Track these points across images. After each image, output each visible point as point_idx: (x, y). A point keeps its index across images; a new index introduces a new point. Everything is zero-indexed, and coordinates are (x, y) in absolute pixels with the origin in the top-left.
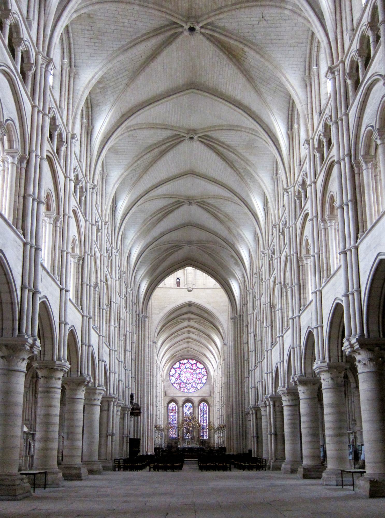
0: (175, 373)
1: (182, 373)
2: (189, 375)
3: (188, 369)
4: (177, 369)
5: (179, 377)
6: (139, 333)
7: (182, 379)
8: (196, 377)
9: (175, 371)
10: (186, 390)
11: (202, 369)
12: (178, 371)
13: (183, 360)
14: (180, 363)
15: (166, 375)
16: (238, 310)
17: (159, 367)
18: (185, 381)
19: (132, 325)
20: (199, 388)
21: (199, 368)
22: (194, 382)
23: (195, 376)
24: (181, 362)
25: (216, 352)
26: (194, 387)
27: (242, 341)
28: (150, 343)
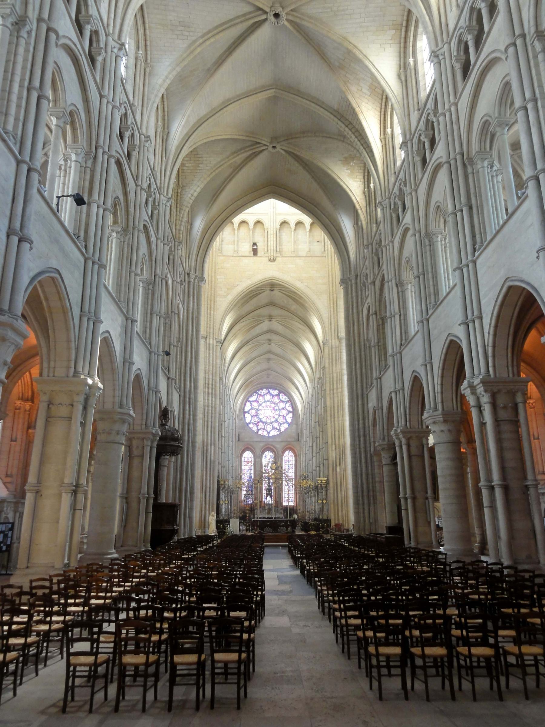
0: (252, 408)
1: (260, 408)
3: (268, 403)
4: (253, 403)
5: (257, 415)
6: (188, 307)
7: (261, 417)
9: (251, 405)
10: (265, 434)
12: (255, 405)
13: (262, 389)
14: (258, 394)
15: (240, 411)
16: (352, 269)
17: (228, 393)
18: (264, 420)
19: (173, 281)
20: (282, 429)
21: (283, 401)
22: (276, 421)
23: (277, 412)
24: (259, 393)
25: (307, 372)
26: (276, 429)
27: (361, 319)
28: (211, 342)
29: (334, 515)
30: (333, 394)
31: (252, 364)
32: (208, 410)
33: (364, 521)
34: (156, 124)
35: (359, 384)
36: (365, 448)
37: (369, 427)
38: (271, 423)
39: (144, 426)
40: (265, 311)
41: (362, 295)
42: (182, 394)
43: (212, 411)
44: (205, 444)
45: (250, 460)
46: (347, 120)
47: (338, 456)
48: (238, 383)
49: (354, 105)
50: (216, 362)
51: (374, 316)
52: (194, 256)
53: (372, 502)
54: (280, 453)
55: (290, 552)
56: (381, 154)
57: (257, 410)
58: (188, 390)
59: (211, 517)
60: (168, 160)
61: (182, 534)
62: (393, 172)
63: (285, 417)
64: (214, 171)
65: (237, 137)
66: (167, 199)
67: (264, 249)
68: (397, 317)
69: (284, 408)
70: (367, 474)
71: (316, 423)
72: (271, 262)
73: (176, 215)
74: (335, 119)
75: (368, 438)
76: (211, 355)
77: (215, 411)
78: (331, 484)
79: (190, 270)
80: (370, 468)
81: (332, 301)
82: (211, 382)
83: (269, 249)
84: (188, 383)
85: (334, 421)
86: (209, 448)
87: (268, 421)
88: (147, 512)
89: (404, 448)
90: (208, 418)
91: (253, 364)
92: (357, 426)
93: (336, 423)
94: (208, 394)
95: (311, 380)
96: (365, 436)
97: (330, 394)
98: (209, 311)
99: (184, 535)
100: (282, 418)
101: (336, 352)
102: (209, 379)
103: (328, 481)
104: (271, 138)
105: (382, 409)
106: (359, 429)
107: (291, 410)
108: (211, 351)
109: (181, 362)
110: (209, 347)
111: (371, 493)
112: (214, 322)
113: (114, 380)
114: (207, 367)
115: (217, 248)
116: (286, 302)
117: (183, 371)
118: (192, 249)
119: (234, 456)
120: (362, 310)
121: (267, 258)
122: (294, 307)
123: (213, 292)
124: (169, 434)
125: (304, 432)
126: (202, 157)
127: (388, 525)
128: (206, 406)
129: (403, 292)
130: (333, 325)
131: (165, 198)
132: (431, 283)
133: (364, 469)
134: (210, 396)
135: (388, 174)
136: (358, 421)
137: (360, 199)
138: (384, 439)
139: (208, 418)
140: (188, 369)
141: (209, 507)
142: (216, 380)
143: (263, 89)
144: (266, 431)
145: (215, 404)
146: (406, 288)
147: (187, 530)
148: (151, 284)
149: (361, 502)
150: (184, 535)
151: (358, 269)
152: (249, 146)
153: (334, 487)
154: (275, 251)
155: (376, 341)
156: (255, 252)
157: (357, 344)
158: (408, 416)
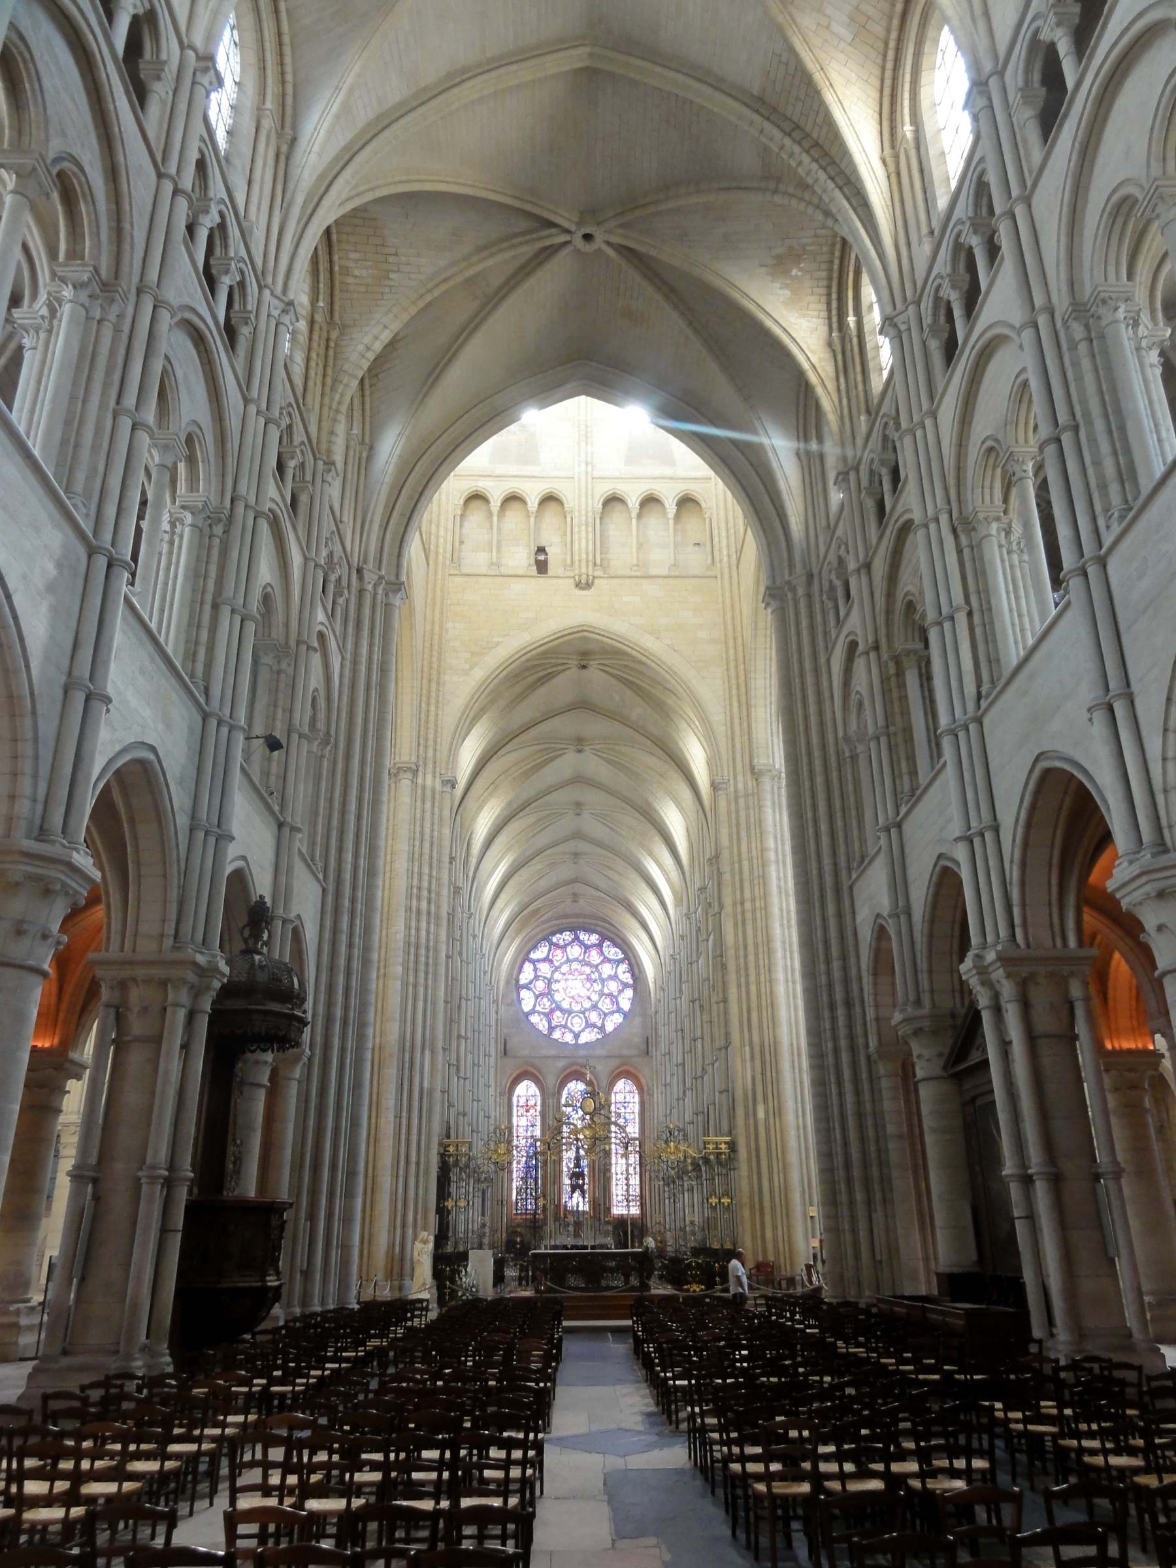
0: (536, 977)
1: (557, 976)
2: (578, 984)
3: (575, 965)
4: (540, 966)
5: (548, 993)
7: (557, 997)
8: (601, 990)
9: (536, 969)
10: (569, 1038)
11: (619, 962)
12: (545, 968)
13: (561, 932)
14: (551, 944)
15: (508, 982)
18: (565, 1005)
20: (609, 1027)
21: (609, 961)
22: (595, 1007)
23: (597, 987)
24: (554, 940)
25: (668, 880)
26: (594, 1026)
27: (825, 684)
28: (429, 782)
29: (754, 1237)
30: (743, 913)
31: (536, 866)
32: (417, 955)
33: (857, 1256)
34: (259, 109)
35: (827, 861)
36: (851, 1037)
37: (860, 978)
38: (583, 1013)
39: (169, 942)
40: (564, 726)
41: (824, 623)
42: (331, 888)
43: (427, 958)
44: (408, 1044)
45: (531, 1103)
46: (786, 118)
47: (759, 1077)
48: (502, 911)
49: (811, 65)
50: (440, 833)
51: (873, 655)
52: (376, 527)
53: (878, 1196)
54: (604, 1084)
55: (638, 1344)
56: (887, 196)
57: (549, 981)
59: (418, 1245)
60: (290, 205)
61: (316, 1301)
62: (925, 230)
63: (616, 997)
64: (430, 291)
65: (492, 196)
66: (281, 306)
67: (565, 560)
68: (961, 618)
69: (614, 977)
70: (860, 1116)
71: (693, 1002)
72: (582, 589)
73: (323, 395)
74: (756, 117)
75: (858, 1009)
76: (428, 815)
77: (436, 958)
78: (742, 1153)
79: (365, 562)
80: (867, 1096)
81: (734, 681)
82: (425, 884)
83: (576, 558)
84: (349, 857)
85: (747, 984)
86: (418, 1056)
87: (576, 1008)
88: (164, 1231)
90: (416, 977)
91: (539, 867)
92: (824, 978)
93: (753, 988)
94: (419, 912)
95: (678, 902)
96: (848, 1004)
97: (735, 916)
98: (423, 705)
99: (323, 1302)
100: (608, 1001)
101: (747, 808)
102: (420, 874)
103: (732, 1146)
104: (582, 213)
105: (909, 915)
106: (830, 986)
107: (631, 982)
108: (428, 805)
109: (331, 801)
110: (424, 794)
111: (875, 1172)
112: (436, 732)
113: (15, 740)
114: (417, 843)
115: (449, 555)
116: (617, 698)
117: (335, 823)
118: (372, 507)
119: (492, 1091)
120: (828, 660)
121: (572, 580)
122: (638, 710)
123: (435, 659)
124: (262, 977)
125: (662, 1031)
126: (396, 254)
127: (948, 1270)
128: (412, 946)
129: (977, 548)
131: (276, 302)
133: (849, 1098)
134: (424, 918)
135: (909, 244)
136: (828, 962)
137: (820, 360)
138: (918, 1002)
139: (416, 977)
140: (352, 819)
141: (415, 1219)
142: (438, 879)
143: (559, 44)
144: (571, 1031)
145: (436, 942)
146: (984, 533)
147: (332, 1287)
148: (220, 520)
149: (844, 1198)
150: (323, 1303)
151: (813, 559)
152: (522, 234)
153: (749, 1160)
154: (591, 564)
155: (881, 722)
156: (542, 567)
157: (817, 753)
158: (1016, 911)
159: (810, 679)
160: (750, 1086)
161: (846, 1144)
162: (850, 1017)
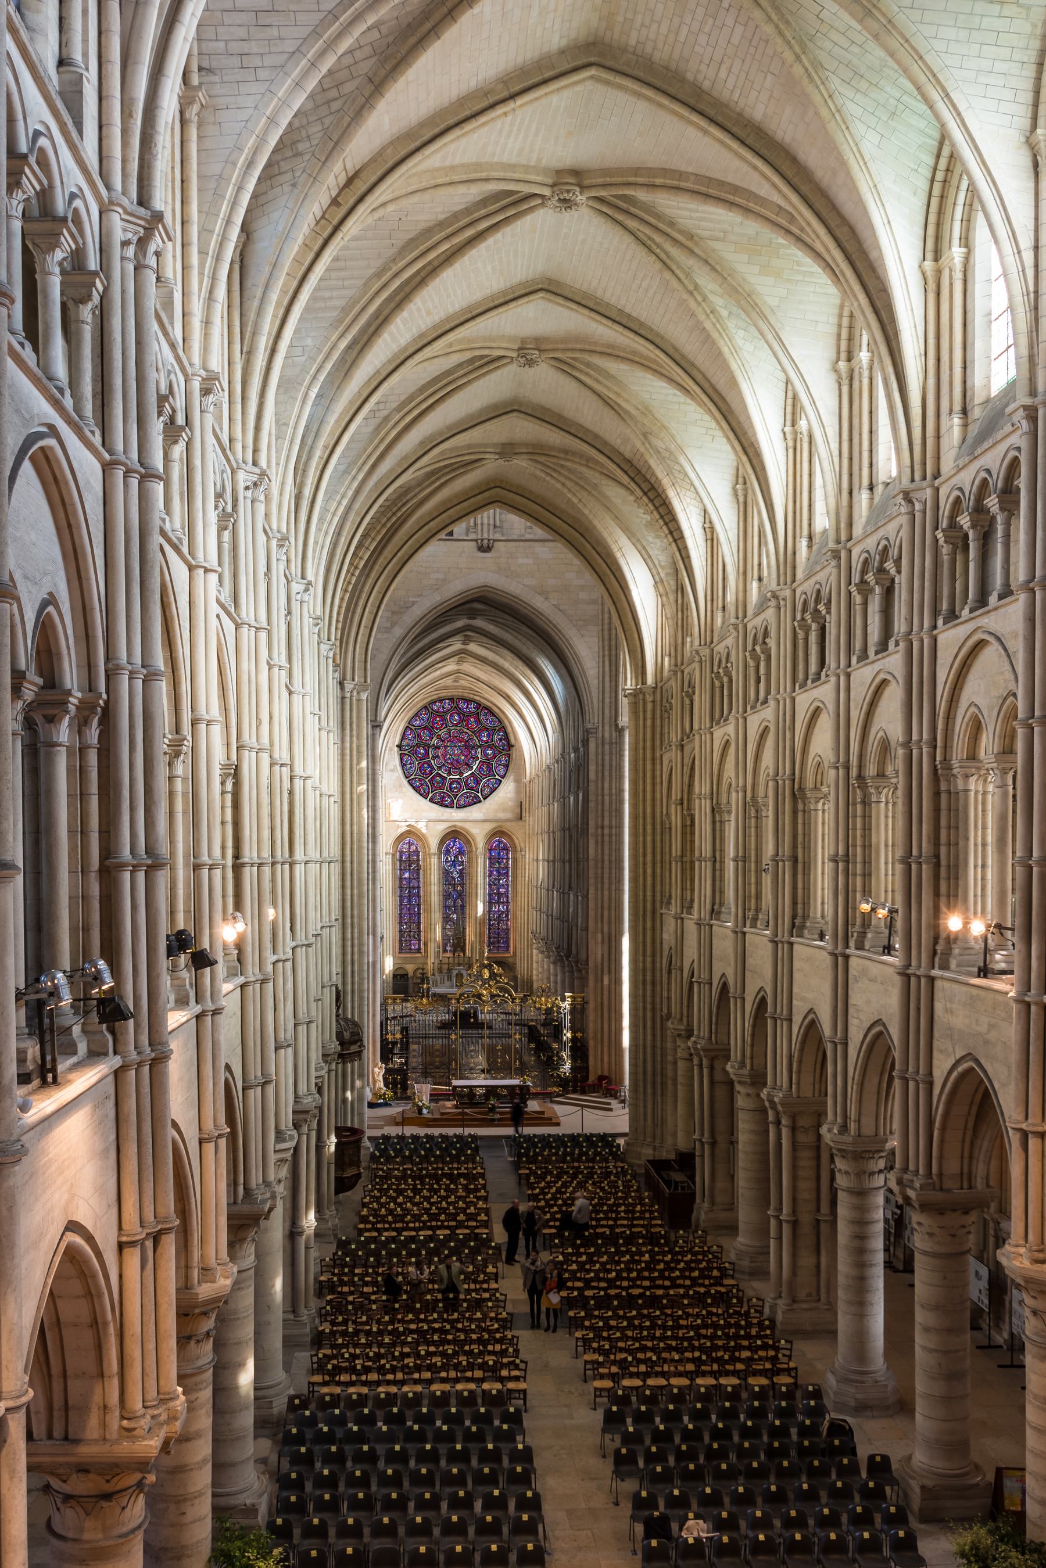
27: (658, 773)
30: (603, 835)
33: (645, 1120)
35: (649, 894)
36: (653, 1003)
46: (647, 480)
56: (704, 559)
58: (349, 904)
70: (654, 1047)
75: (658, 988)
78: (591, 1005)
79: (344, 679)
80: (659, 1038)
81: (606, 643)
85: (602, 889)
89: (705, 1071)
93: (606, 893)
96: (653, 983)
100: (484, 767)
101: (611, 753)
106: (644, 970)
111: (659, 1080)
130: (607, 695)
132: (753, 880)
133: (649, 1037)
136: (644, 955)
137: (667, 574)
138: (681, 1019)
157: (649, 820)
159: (649, 767)
160: (599, 960)
161: (645, 1061)
162: (653, 991)
